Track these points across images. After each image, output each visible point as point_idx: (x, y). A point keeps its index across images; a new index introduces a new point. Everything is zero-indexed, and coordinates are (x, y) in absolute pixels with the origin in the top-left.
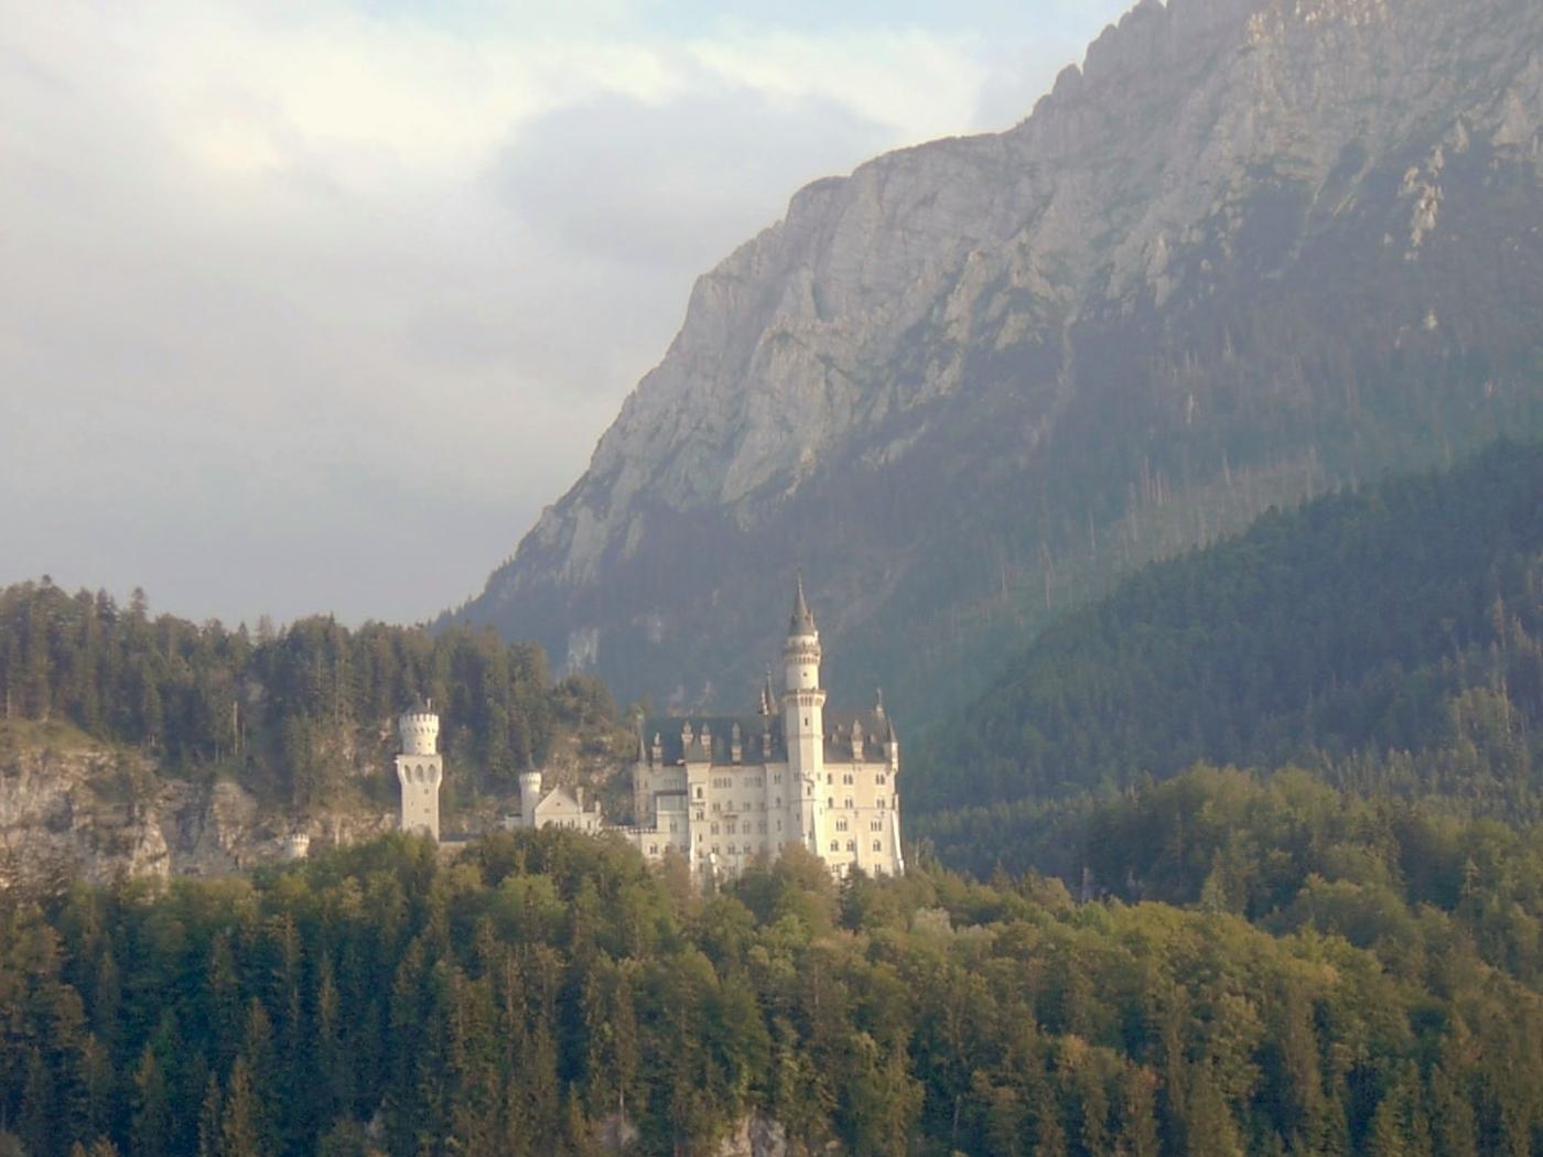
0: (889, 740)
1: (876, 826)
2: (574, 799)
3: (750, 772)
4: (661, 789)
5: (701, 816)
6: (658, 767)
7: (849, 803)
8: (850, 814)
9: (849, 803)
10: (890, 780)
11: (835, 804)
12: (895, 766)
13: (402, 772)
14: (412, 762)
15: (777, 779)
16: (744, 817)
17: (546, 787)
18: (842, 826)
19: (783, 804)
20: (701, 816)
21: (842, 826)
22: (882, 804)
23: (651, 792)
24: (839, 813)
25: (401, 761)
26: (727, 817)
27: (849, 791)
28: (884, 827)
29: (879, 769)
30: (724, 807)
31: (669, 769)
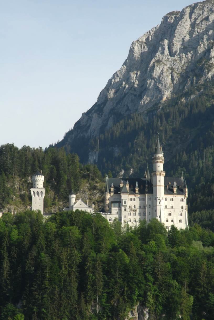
0: (185, 187)
1: (180, 215)
2: (86, 204)
7: (172, 207)
8: (172, 210)
10: (185, 200)
11: (168, 207)
12: (187, 196)
13: (32, 193)
17: (77, 199)
18: (169, 214)
20: (125, 210)
21: (169, 214)
22: (182, 208)
24: (169, 210)
25: (32, 190)
27: (172, 203)
28: (183, 215)
29: (182, 197)
30: (133, 207)
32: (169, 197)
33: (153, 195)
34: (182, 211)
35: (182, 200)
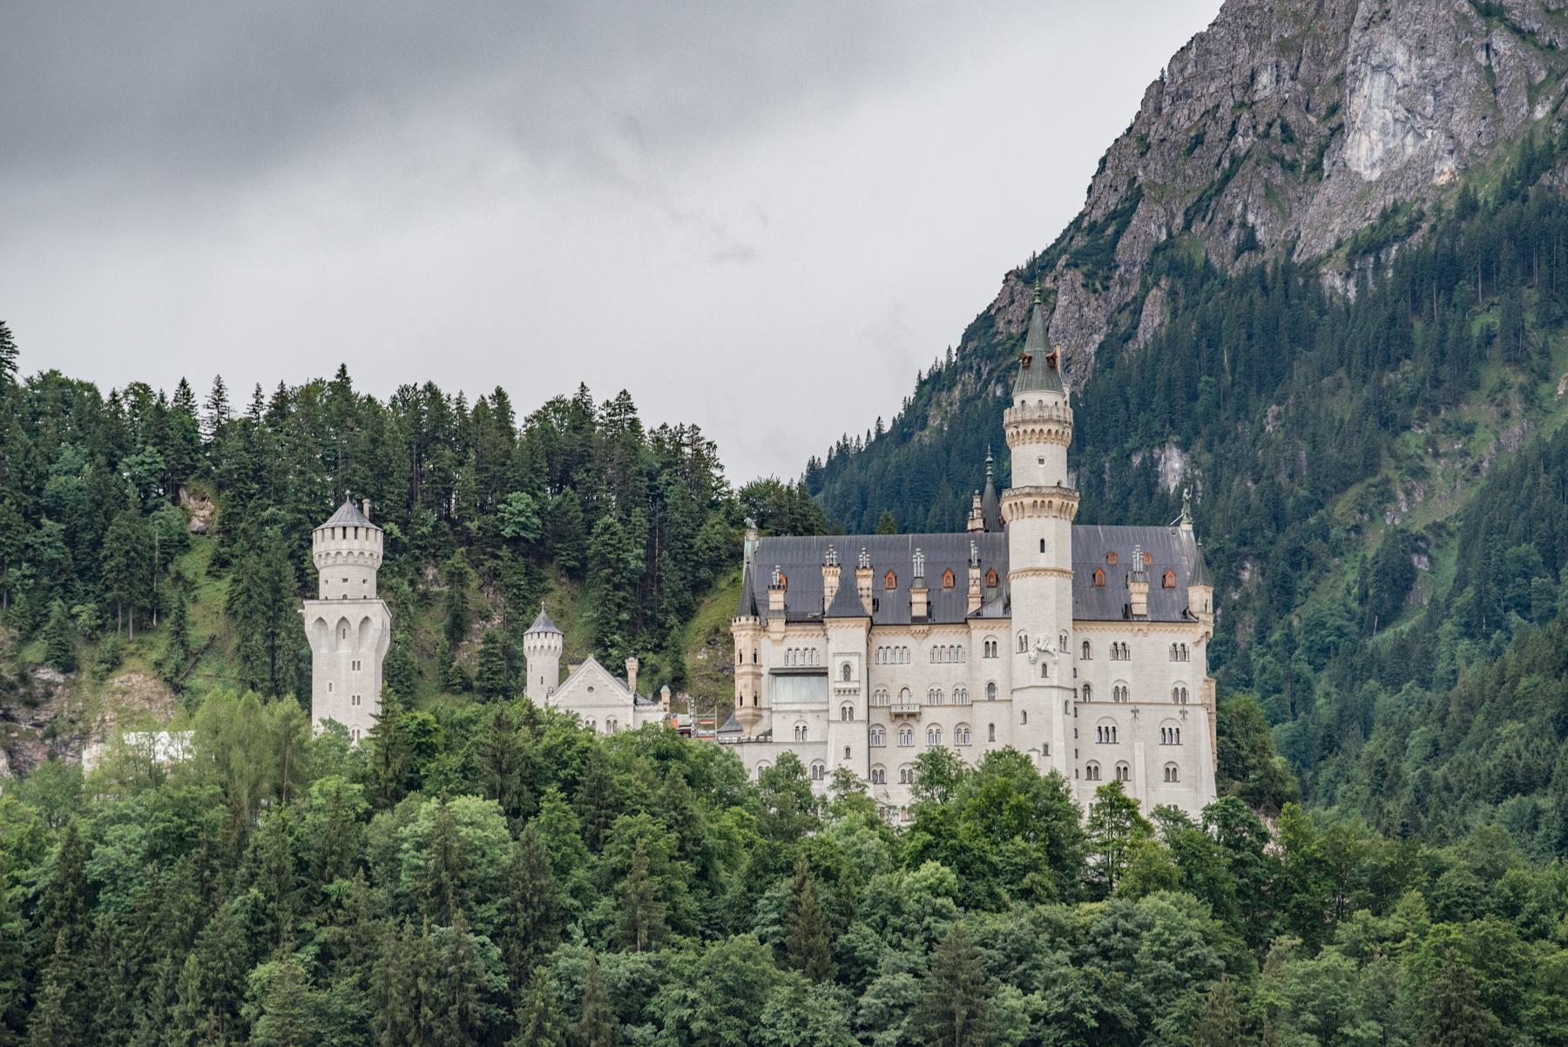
1: (1170, 736)
3: (944, 637)
4: (779, 663)
5: (847, 714)
6: (777, 625)
7: (1120, 694)
8: (1121, 715)
9: (1120, 694)
10: (1199, 655)
11: (1096, 695)
13: (310, 627)
14: (332, 614)
15: (990, 648)
16: (930, 715)
19: (999, 695)
22: (1180, 695)
23: (765, 671)
26: (898, 716)
27: (1121, 672)
31: (797, 630)
32: (1103, 637)
33: (1009, 627)
34: (1179, 717)
35: (1179, 652)
